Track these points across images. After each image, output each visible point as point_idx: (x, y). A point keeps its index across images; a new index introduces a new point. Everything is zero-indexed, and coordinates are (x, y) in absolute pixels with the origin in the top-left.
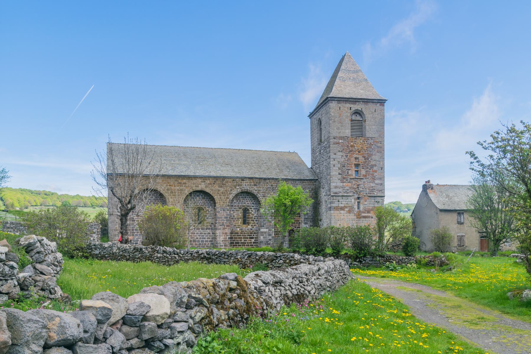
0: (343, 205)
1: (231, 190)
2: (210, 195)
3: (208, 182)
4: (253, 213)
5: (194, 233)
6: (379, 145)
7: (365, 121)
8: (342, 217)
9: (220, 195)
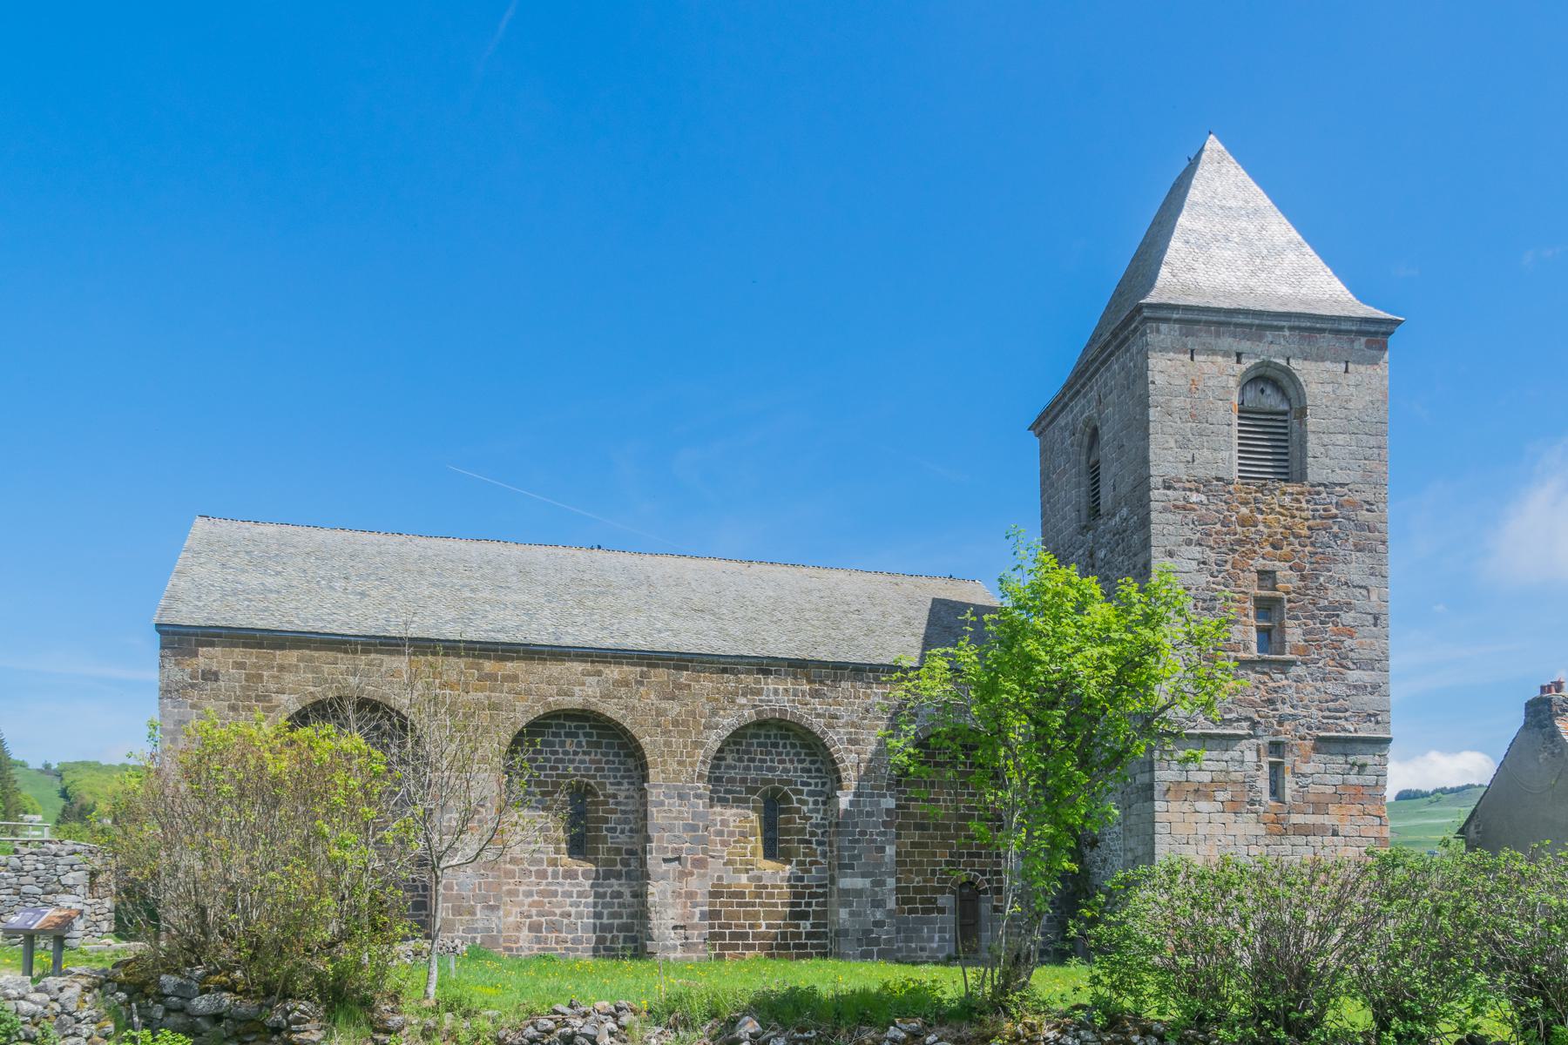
0: (1206, 777)
1: (714, 713)
2: (625, 731)
3: (613, 672)
4: (806, 807)
5: (555, 894)
6: (1363, 515)
7: (1302, 413)
8: (1203, 830)
9: (666, 732)
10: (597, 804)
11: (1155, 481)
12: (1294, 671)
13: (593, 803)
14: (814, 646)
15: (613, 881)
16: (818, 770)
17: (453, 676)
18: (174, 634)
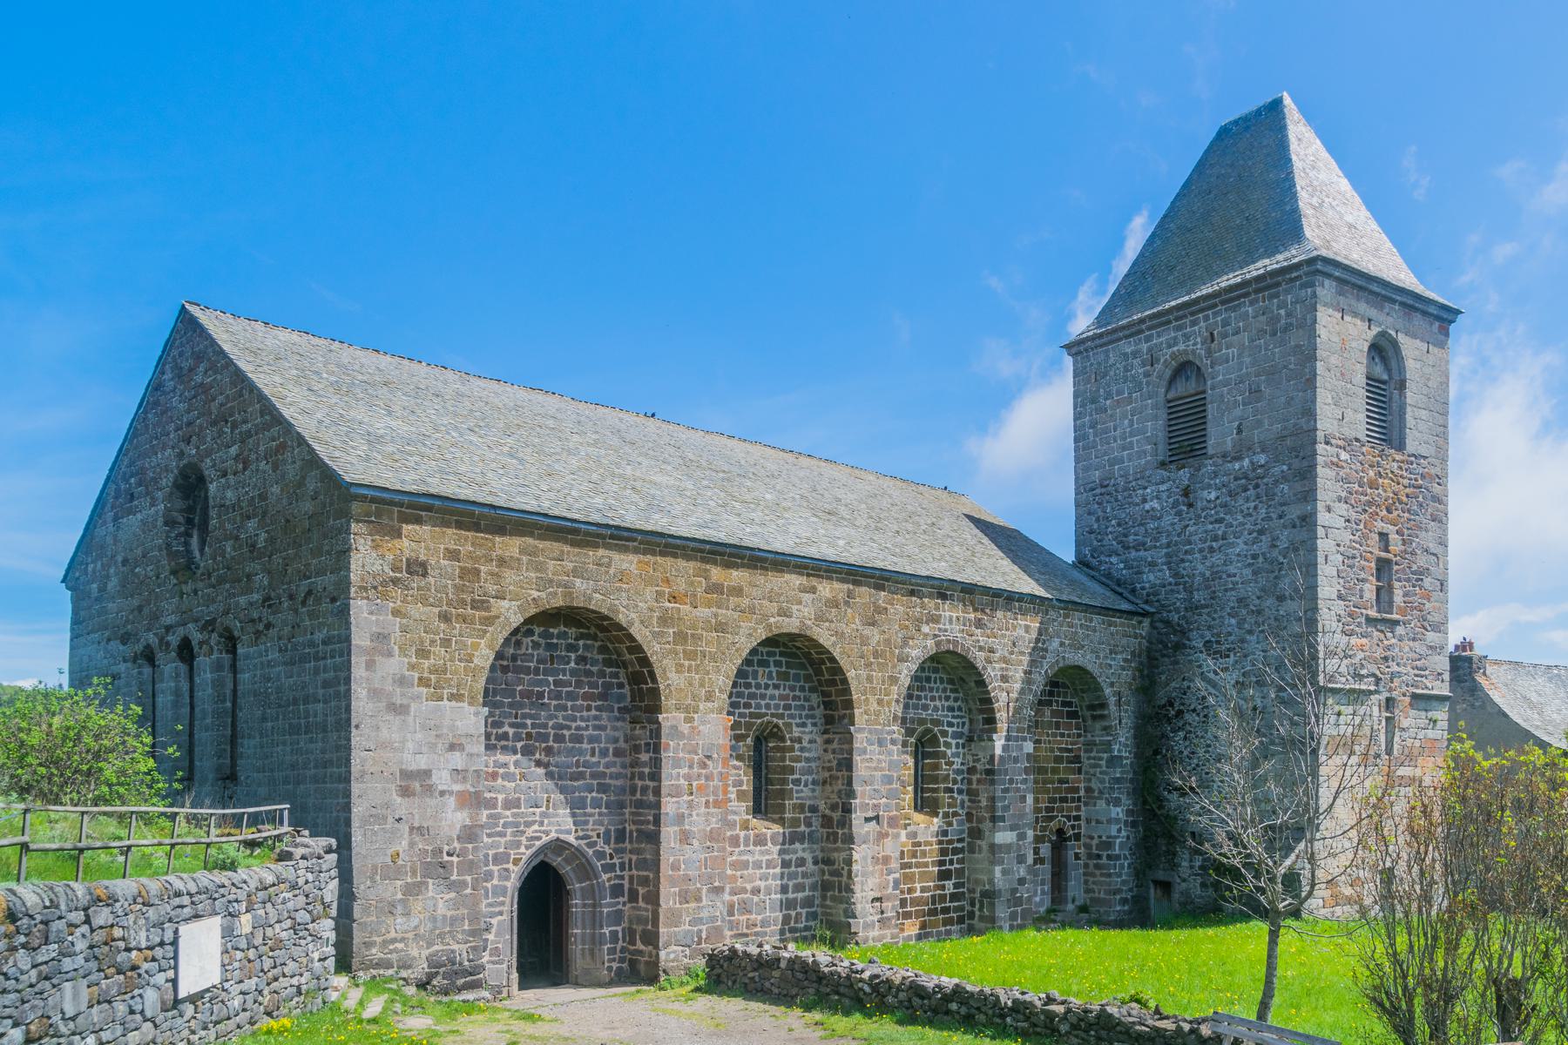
3: (827, 589)
4: (953, 755)
5: (745, 865)
7: (1402, 385)
10: (783, 750)
11: (1320, 435)
12: (1400, 630)
13: (778, 749)
14: (962, 569)
15: (797, 845)
16: (960, 709)
17: (681, 585)
18: (373, 500)
